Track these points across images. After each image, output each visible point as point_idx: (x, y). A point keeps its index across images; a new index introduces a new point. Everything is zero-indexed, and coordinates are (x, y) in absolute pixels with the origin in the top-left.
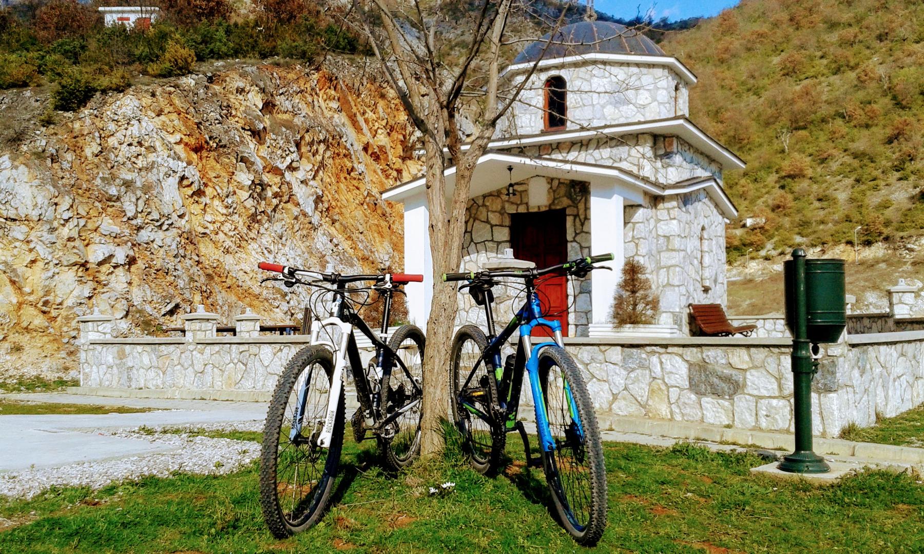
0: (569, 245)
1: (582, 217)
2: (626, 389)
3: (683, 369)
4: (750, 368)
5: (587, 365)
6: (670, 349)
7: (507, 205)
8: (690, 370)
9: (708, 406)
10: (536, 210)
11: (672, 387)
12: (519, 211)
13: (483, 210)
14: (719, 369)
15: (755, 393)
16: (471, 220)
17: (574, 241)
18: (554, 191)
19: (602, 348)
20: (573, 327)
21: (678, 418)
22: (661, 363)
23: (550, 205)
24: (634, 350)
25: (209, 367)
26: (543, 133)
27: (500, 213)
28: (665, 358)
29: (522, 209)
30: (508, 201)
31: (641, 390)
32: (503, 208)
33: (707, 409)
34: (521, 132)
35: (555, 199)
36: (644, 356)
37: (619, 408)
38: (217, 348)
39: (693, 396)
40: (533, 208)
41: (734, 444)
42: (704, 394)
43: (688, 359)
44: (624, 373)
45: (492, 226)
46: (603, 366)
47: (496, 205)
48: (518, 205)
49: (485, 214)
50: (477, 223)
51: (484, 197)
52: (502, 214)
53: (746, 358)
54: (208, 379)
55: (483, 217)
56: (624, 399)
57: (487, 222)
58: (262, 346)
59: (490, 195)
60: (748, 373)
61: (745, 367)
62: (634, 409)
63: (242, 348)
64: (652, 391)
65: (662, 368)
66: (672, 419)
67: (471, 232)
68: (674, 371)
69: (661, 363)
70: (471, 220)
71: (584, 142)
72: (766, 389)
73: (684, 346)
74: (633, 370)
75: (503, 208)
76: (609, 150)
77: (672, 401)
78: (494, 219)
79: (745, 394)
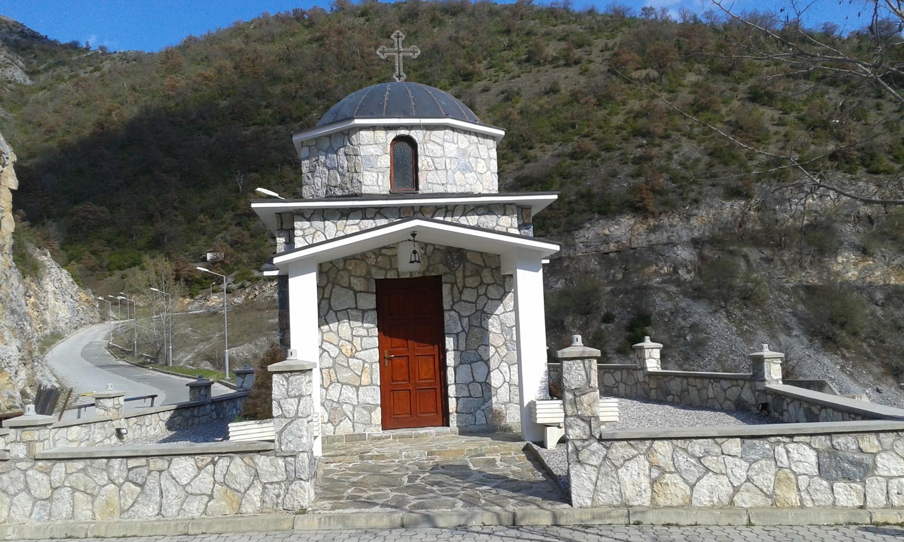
0: (446, 314)
1: (460, 285)
2: (748, 480)
3: (812, 457)
4: (879, 452)
5: (699, 458)
6: (796, 439)
7: (373, 270)
8: (818, 457)
9: (840, 490)
10: (408, 276)
11: (800, 475)
12: (388, 277)
13: (345, 274)
14: (849, 455)
15: (886, 473)
16: (330, 285)
17: (452, 309)
18: (429, 258)
19: (719, 440)
20: (454, 399)
21: (809, 504)
22: (788, 452)
23: (424, 271)
24: (756, 441)
25: (66, 493)
26: (392, 195)
27: (364, 277)
28: (791, 447)
29: (391, 275)
30: (374, 266)
31: (766, 478)
32: (369, 273)
33: (839, 493)
34: (365, 190)
35: (429, 265)
36: (767, 446)
37: (743, 501)
38: (80, 465)
39: (825, 483)
40: (404, 273)
41: (836, 524)
42: (836, 480)
43: (817, 446)
44: (745, 465)
45: (355, 293)
46: (720, 459)
47: (362, 270)
48: (387, 271)
49: (346, 279)
50: (336, 290)
51: (345, 259)
52: (368, 280)
53: (876, 443)
54: (63, 508)
55: (344, 281)
56: (748, 491)
57: (350, 287)
58: (175, 459)
59: (353, 258)
60: (878, 456)
61: (874, 451)
62: (760, 500)
63: (132, 463)
64: (778, 481)
65: (788, 457)
66: (802, 506)
67: (329, 299)
68: (803, 459)
69: (788, 452)
70: (330, 285)
71: (449, 208)
72: (897, 470)
73: (811, 435)
74: (756, 461)
75: (369, 273)
76: (477, 217)
77: (803, 488)
78: (358, 284)
79: (874, 475)
